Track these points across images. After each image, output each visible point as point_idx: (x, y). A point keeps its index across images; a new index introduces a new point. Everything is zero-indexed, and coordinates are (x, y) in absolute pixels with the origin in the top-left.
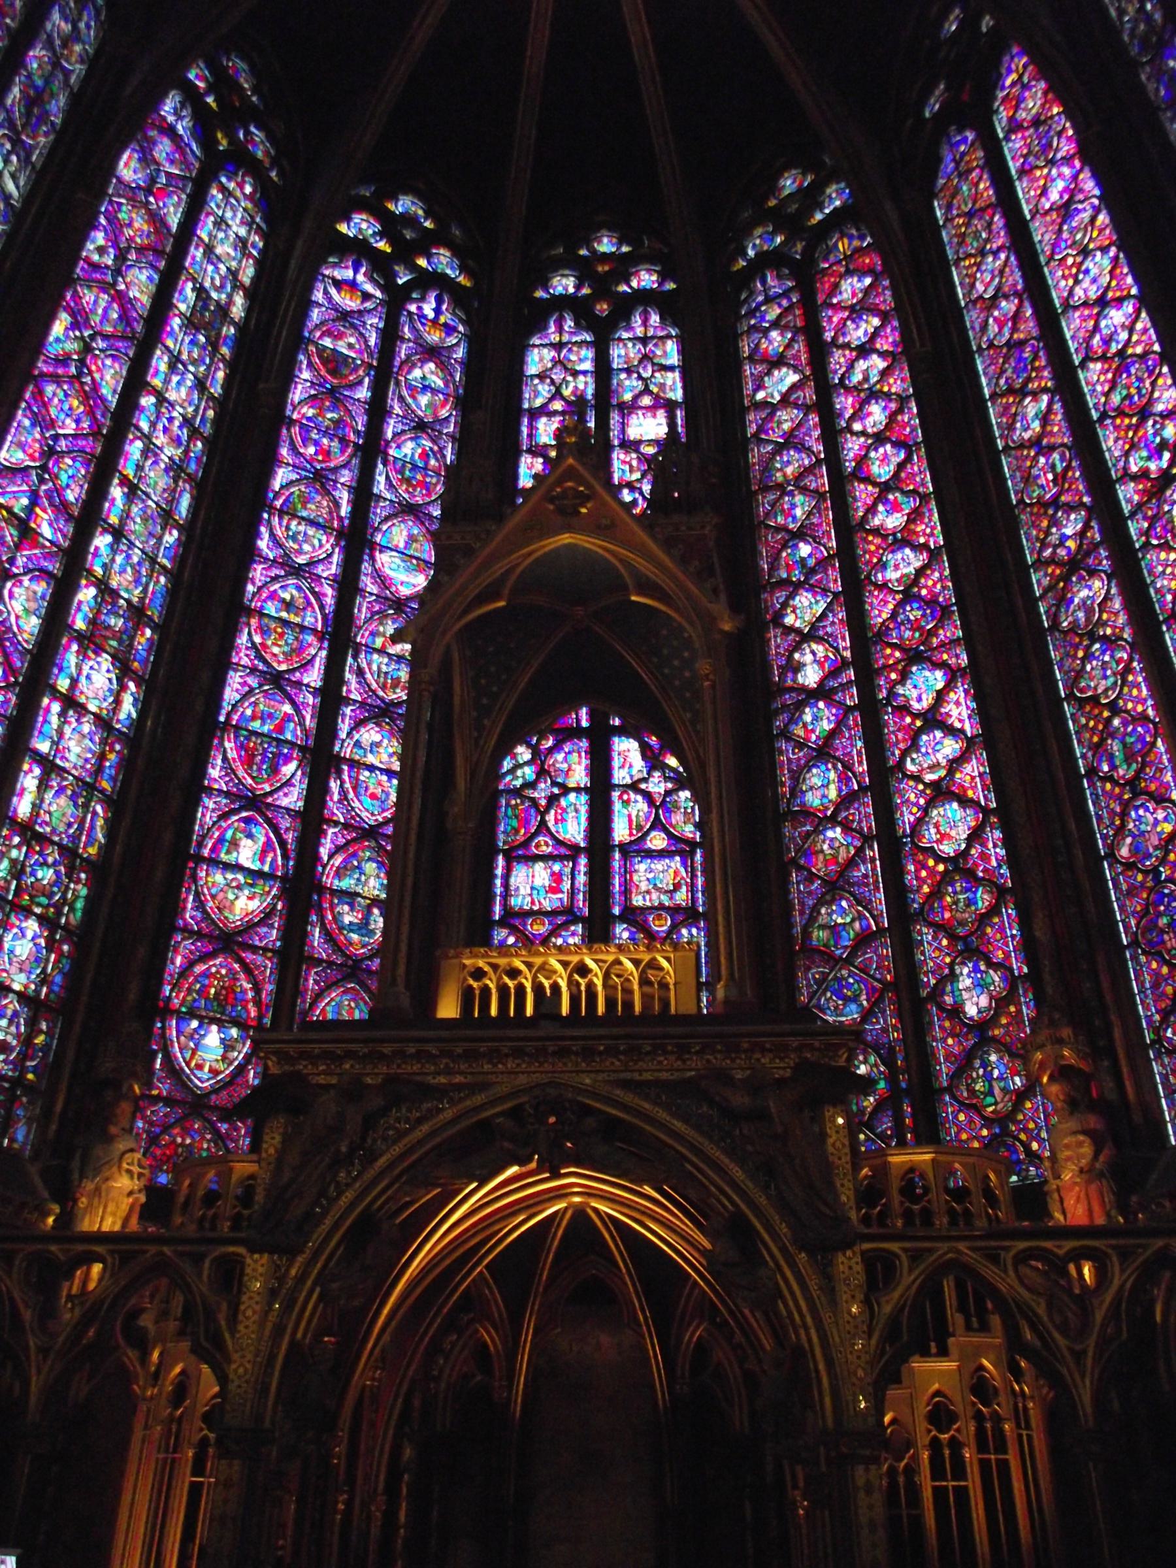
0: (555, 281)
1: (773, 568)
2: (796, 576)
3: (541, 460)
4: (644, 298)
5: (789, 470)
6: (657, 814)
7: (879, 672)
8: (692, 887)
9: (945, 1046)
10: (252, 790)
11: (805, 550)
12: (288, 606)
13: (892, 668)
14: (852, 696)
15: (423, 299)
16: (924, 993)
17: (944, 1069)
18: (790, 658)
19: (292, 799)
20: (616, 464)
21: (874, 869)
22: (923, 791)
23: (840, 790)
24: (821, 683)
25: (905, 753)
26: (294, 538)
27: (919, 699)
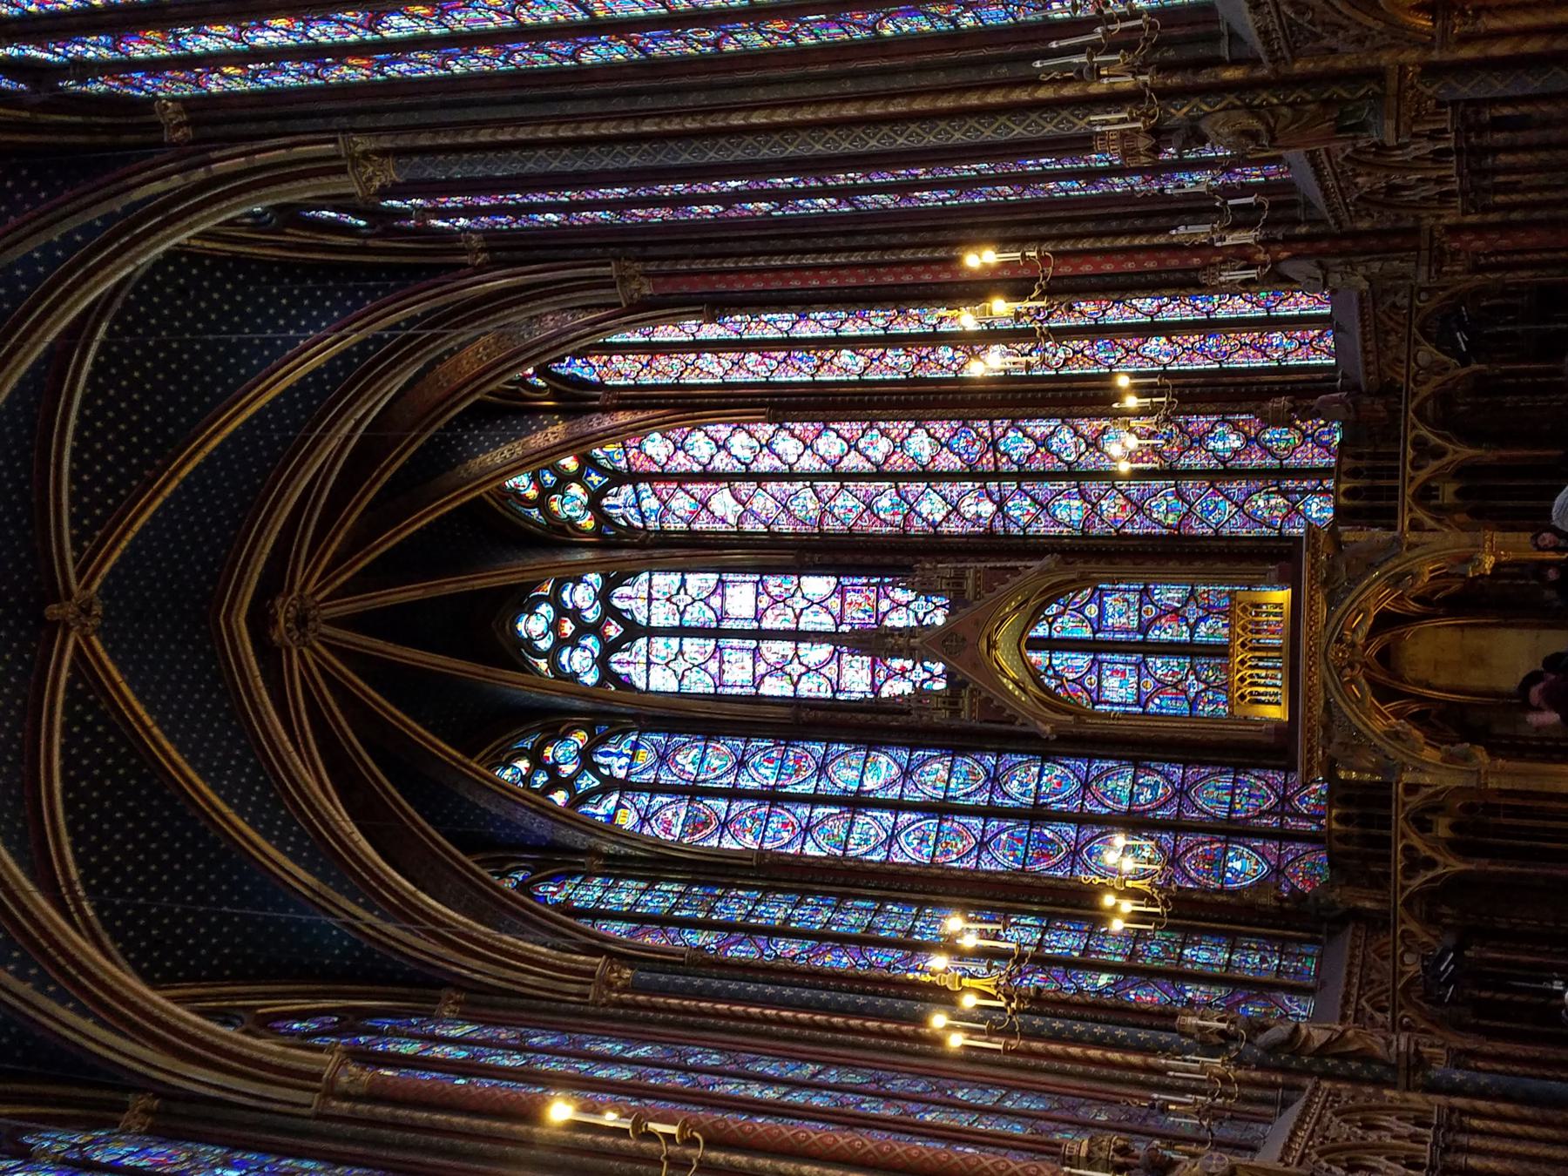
0: (576, 667)
3: (767, 679)
4: (604, 596)
5: (811, 506)
7: (997, 468)
8: (1129, 591)
9: (1256, 460)
10: (1068, 854)
11: (884, 502)
12: (922, 841)
15: (609, 766)
16: (1221, 467)
17: (1269, 460)
19: (1071, 831)
20: (779, 625)
26: (866, 841)
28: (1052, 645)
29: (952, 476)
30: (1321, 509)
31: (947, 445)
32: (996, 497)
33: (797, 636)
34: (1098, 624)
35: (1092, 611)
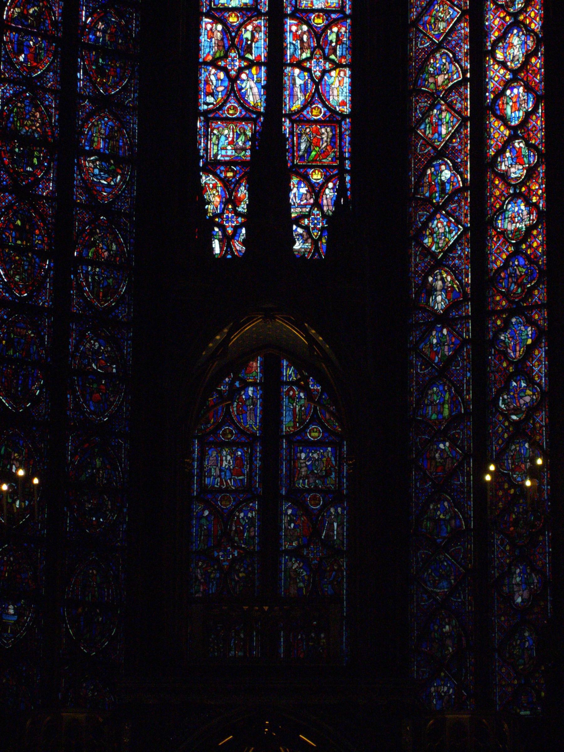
1: (419, 184)
2: (437, 199)
3: (220, 27)
5: (440, 79)
6: (315, 408)
8: (339, 473)
11: (446, 174)
13: (498, 314)
14: (468, 331)
18: (426, 279)
20: (289, 38)
21: (469, 481)
22: (507, 427)
23: (451, 411)
24: (447, 310)
25: (499, 393)
27: (515, 351)
28: (272, 386)
29: (479, 257)
30: (440, 697)
31: (518, 252)
32: (453, 314)
33: (275, 63)
34: (298, 440)
35: (314, 434)
